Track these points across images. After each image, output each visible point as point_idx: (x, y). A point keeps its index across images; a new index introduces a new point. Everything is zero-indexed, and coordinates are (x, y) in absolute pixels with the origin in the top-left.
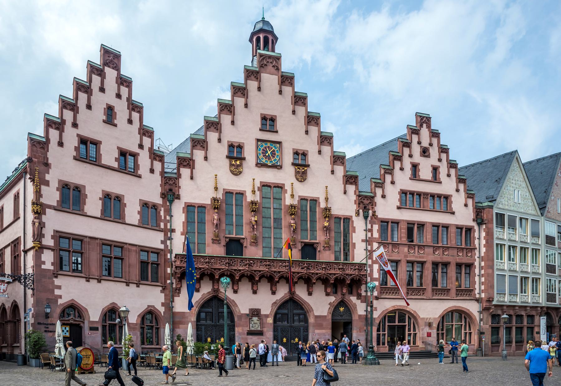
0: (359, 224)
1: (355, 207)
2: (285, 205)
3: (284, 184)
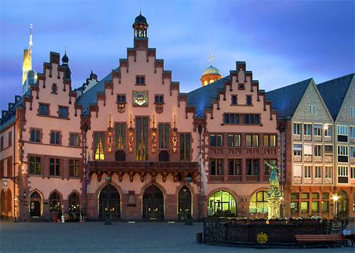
0: (195, 136)
1: (192, 126)
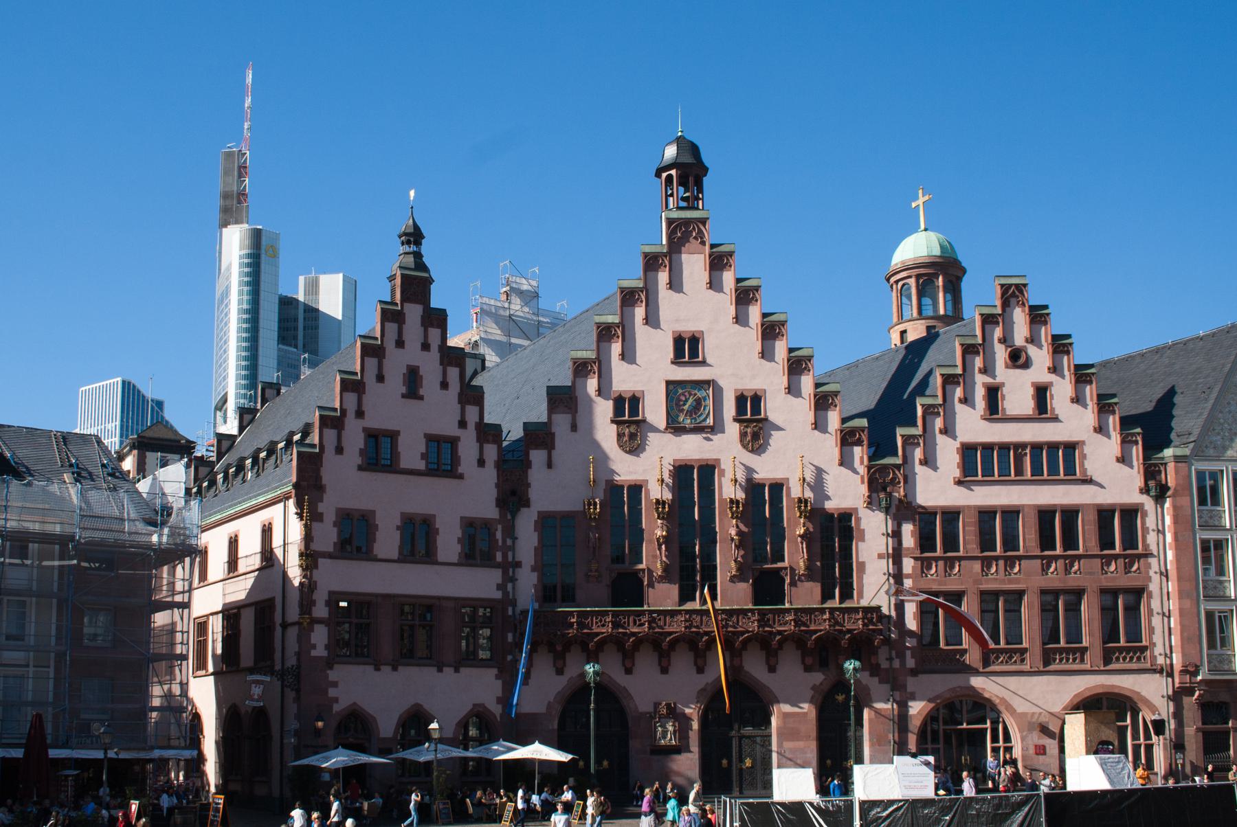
1: (863, 490)
2: (722, 500)
3: (718, 461)
